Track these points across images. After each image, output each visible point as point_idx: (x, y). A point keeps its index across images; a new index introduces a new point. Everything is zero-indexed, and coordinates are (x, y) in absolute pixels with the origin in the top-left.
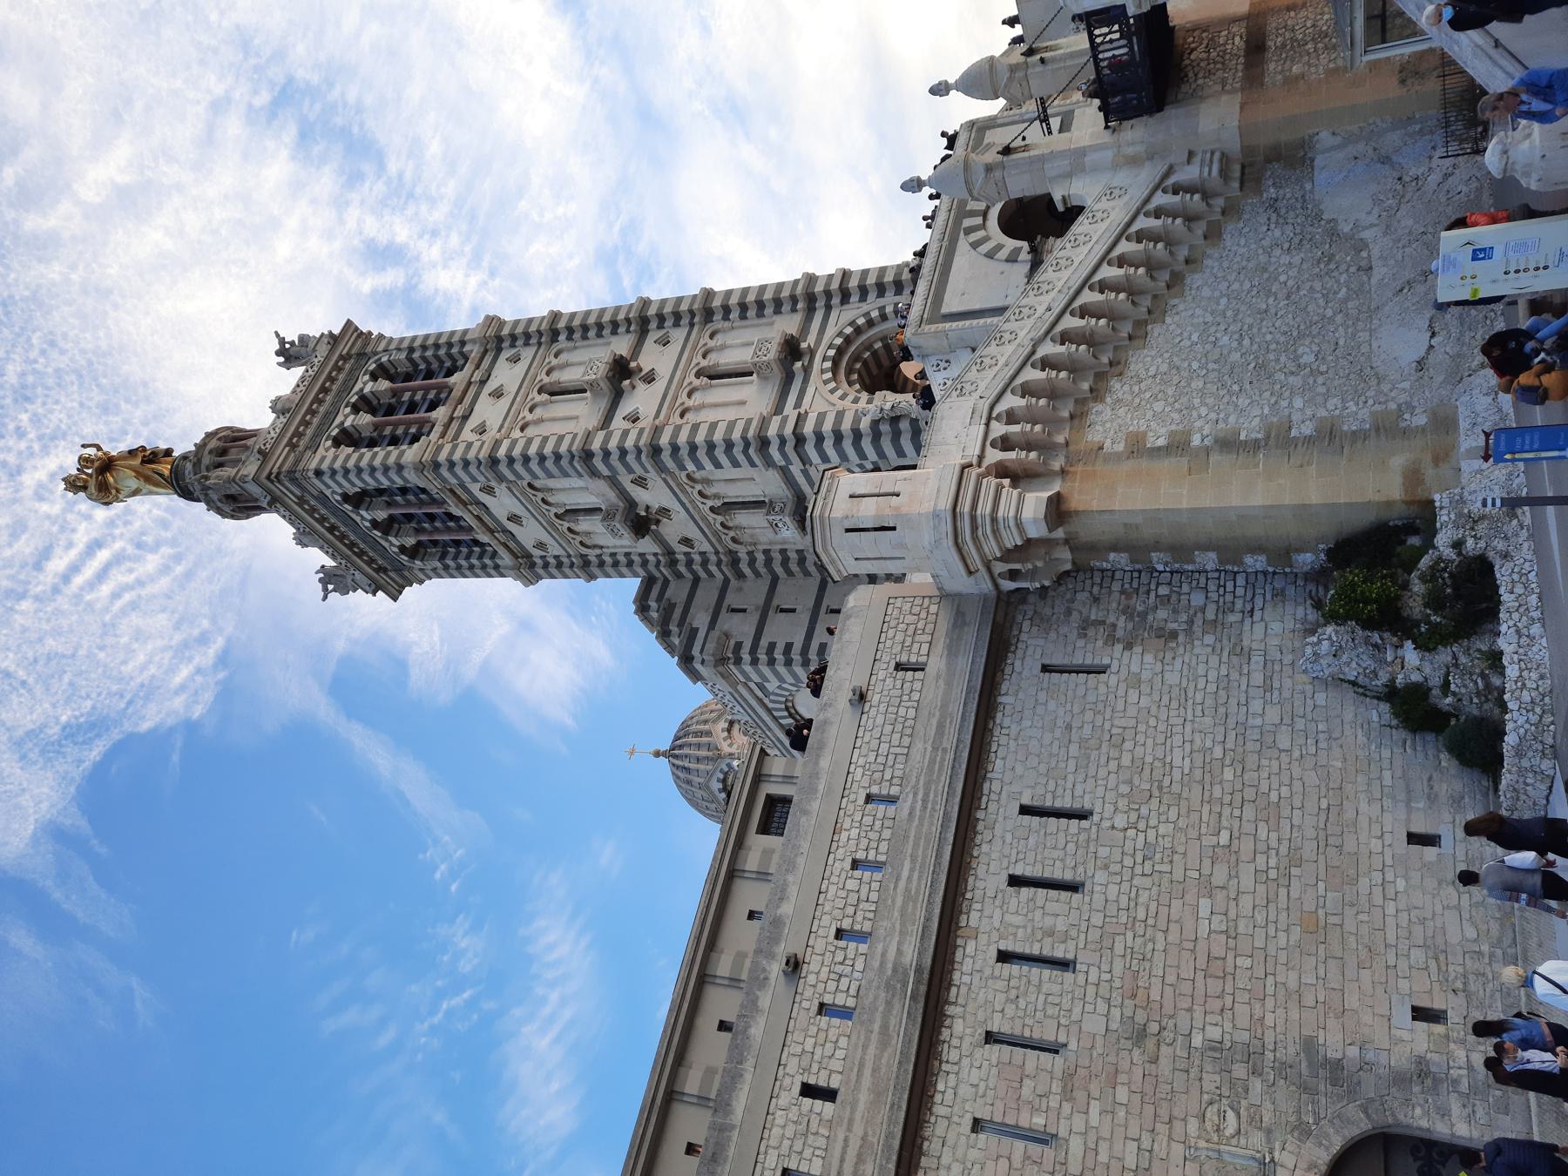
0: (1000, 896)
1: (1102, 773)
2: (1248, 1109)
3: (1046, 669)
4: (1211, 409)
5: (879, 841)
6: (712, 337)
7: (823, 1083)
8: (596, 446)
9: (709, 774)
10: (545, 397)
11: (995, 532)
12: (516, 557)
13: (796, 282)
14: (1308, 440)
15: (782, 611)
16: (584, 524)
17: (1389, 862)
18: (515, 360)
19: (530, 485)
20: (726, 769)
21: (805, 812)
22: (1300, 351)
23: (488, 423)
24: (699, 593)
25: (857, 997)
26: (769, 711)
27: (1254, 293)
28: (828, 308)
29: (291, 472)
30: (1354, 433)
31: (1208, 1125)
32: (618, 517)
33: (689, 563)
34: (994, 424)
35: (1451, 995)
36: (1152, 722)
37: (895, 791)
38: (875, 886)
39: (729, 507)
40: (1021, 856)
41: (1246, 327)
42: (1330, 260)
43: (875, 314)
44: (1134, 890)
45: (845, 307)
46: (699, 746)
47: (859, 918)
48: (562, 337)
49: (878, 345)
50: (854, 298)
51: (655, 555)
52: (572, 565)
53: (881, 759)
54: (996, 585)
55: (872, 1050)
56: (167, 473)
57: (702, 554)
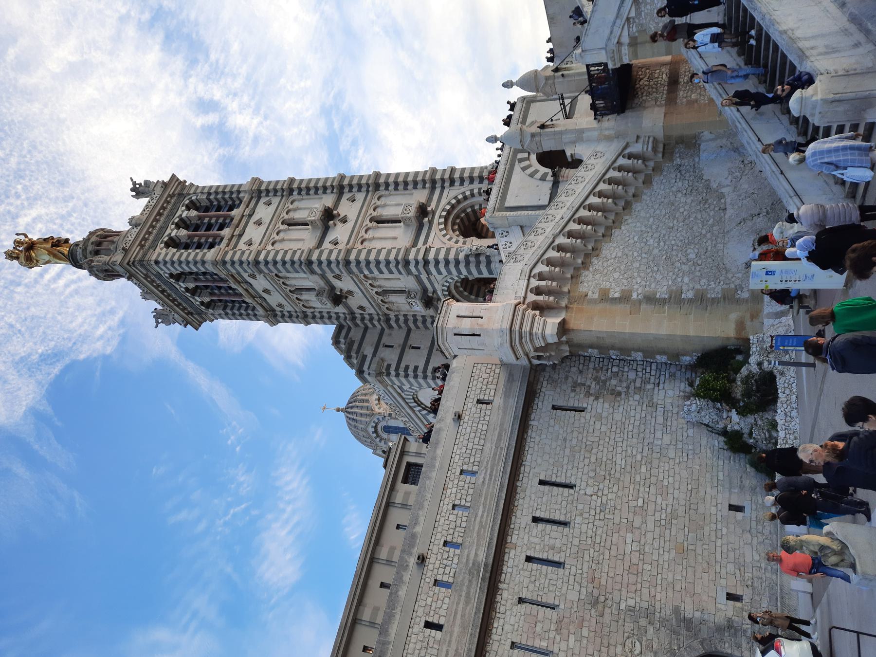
0: (528, 527)
1: (581, 465)
2: (646, 641)
3: (554, 407)
4: (643, 279)
5: (467, 495)
6: (378, 199)
7: (436, 621)
8: (314, 258)
9: (367, 424)
10: (286, 227)
11: (531, 340)
12: (267, 311)
13: (426, 172)
14: (690, 301)
15: (413, 348)
16: (305, 296)
17: (719, 519)
18: (269, 204)
19: (276, 275)
20: (377, 421)
21: (429, 478)
22: (689, 251)
23: (253, 240)
24: (368, 335)
25: (454, 577)
26: (404, 399)
27: (667, 217)
28: (443, 188)
29: (141, 261)
30: (713, 299)
31: (627, 649)
32: (325, 295)
33: (363, 319)
34: (532, 279)
35: (745, 588)
36: (607, 439)
37: (475, 468)
38: (464, 519)
39: (386, 292)
40: (539, 507)
41: (662, 236)
42: (706, 202)
43: (468, 193)
44: (595, 527)
45: (452, 188)
46: (362, 408)
47: (456, 535)
48: (295, 193)
49: (469, 210)
50: (457, 183)
51: (344, 314)
52: (297, 317)
53: (468, 451)
54: (530, 362)
55: (461, 606)
56: (66, 253)
57: (370, 315)
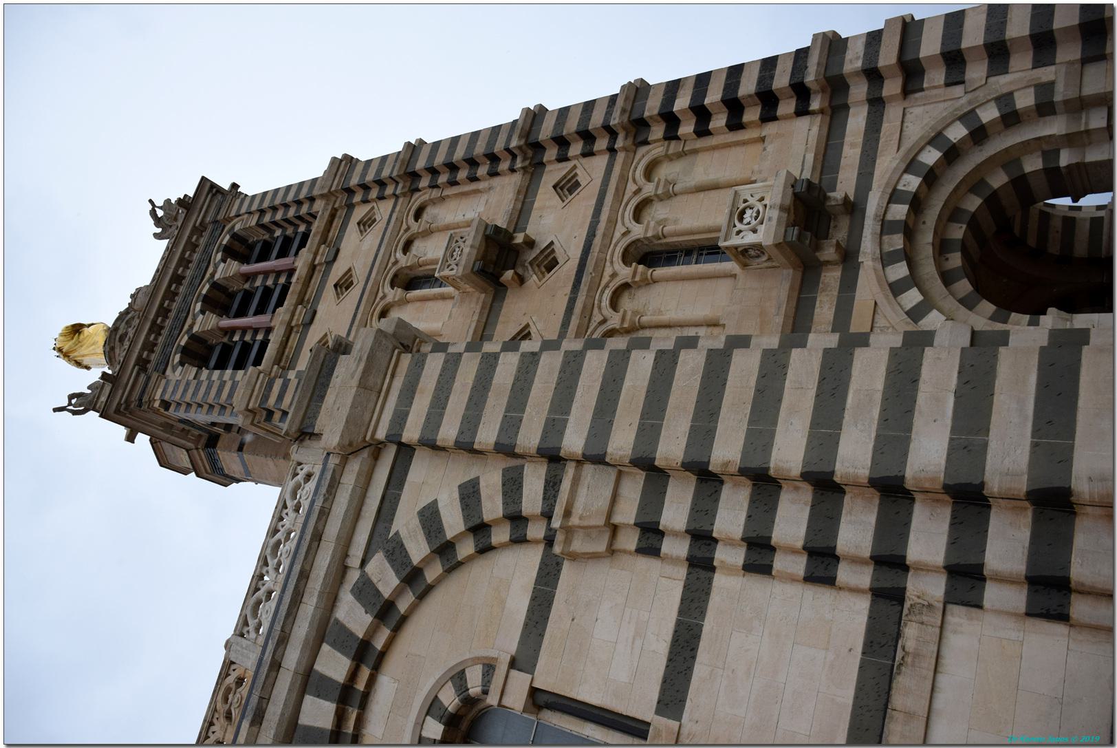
13: (801, 55)
28: (876, 104)
50: (936, 76)
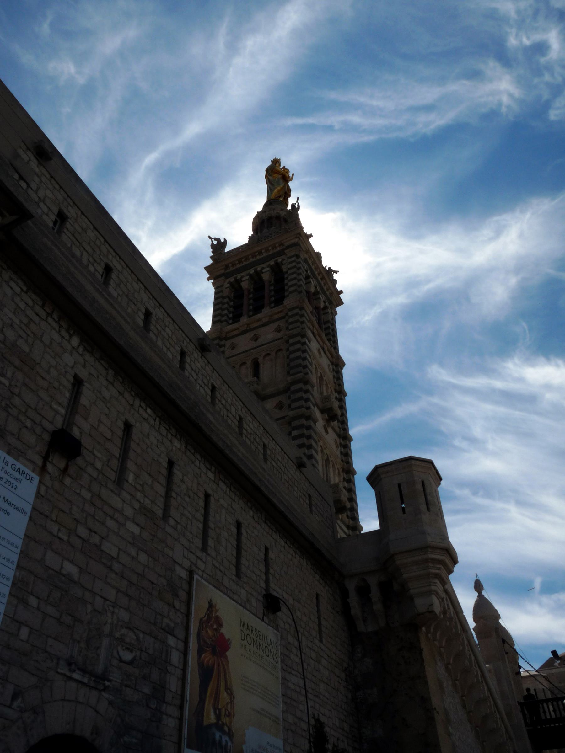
12: (226, 333)
31: (124, 631)
